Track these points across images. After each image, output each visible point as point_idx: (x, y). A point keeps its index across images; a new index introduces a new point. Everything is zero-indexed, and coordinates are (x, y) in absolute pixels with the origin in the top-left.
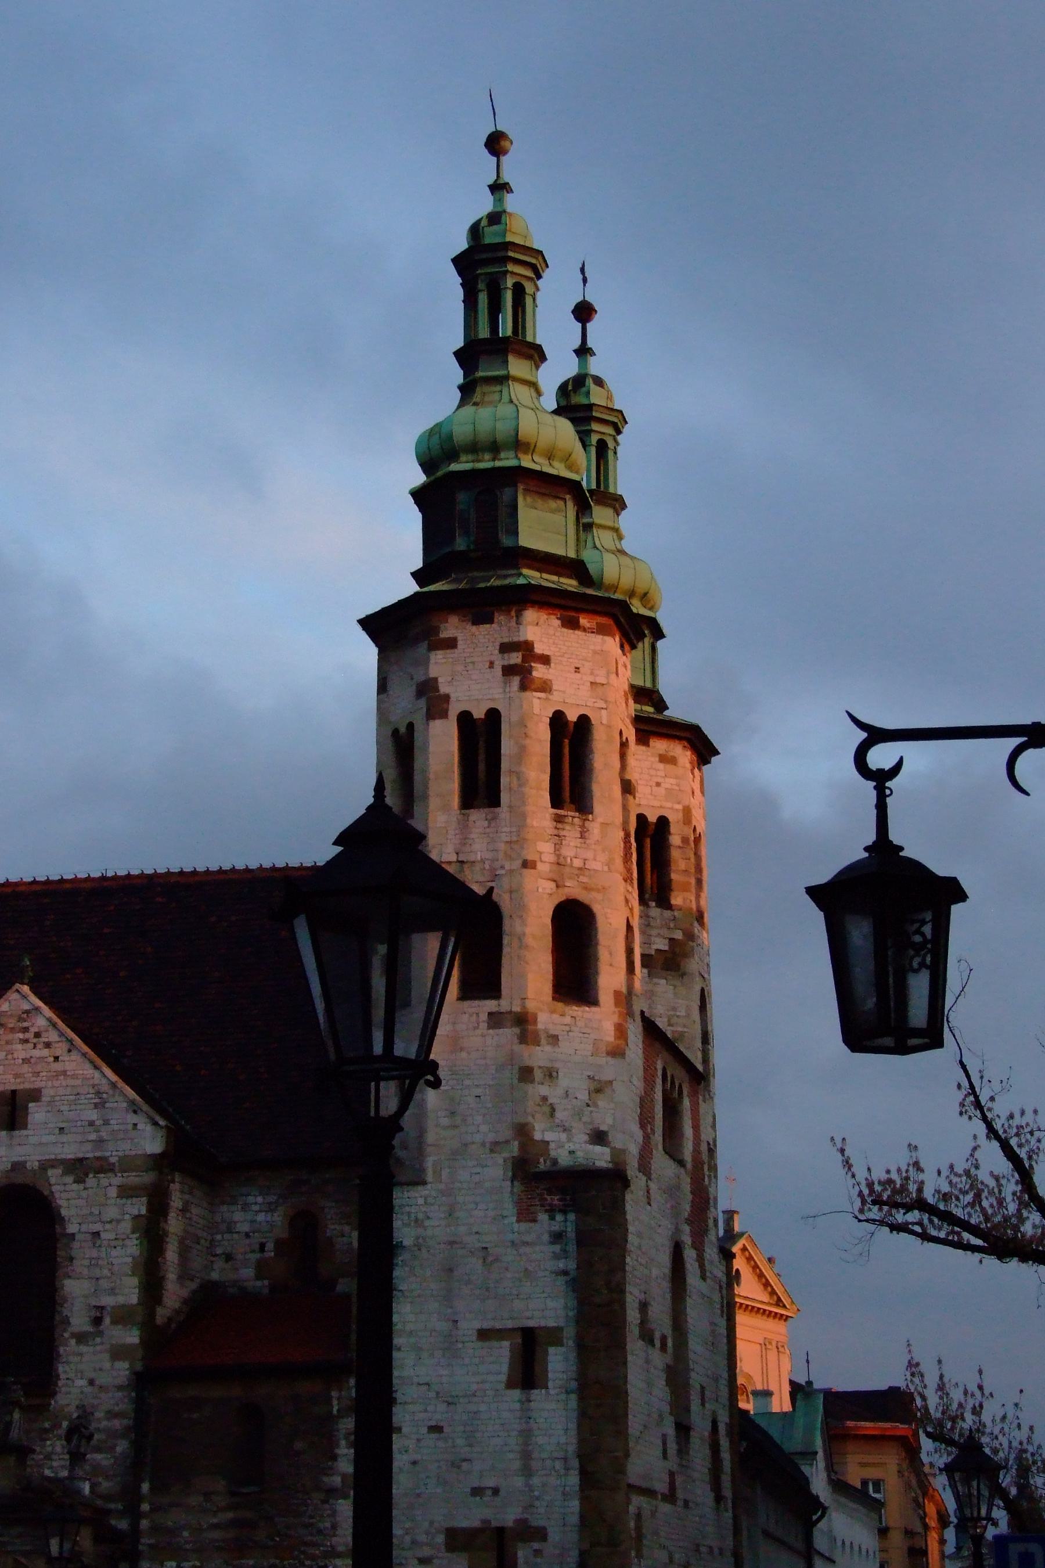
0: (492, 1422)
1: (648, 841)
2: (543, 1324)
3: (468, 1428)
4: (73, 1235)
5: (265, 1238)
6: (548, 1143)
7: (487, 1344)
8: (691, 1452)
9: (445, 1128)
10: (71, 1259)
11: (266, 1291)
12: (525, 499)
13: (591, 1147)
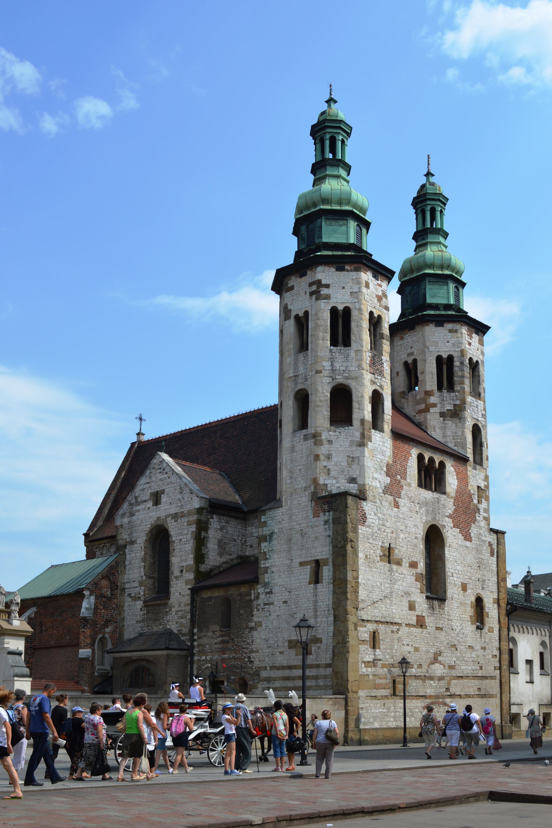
0: (304, 598)
2: (321, 558)
3: (296, 601)
7: (302, 568)
10: (174, 550)
12: (326, 223)
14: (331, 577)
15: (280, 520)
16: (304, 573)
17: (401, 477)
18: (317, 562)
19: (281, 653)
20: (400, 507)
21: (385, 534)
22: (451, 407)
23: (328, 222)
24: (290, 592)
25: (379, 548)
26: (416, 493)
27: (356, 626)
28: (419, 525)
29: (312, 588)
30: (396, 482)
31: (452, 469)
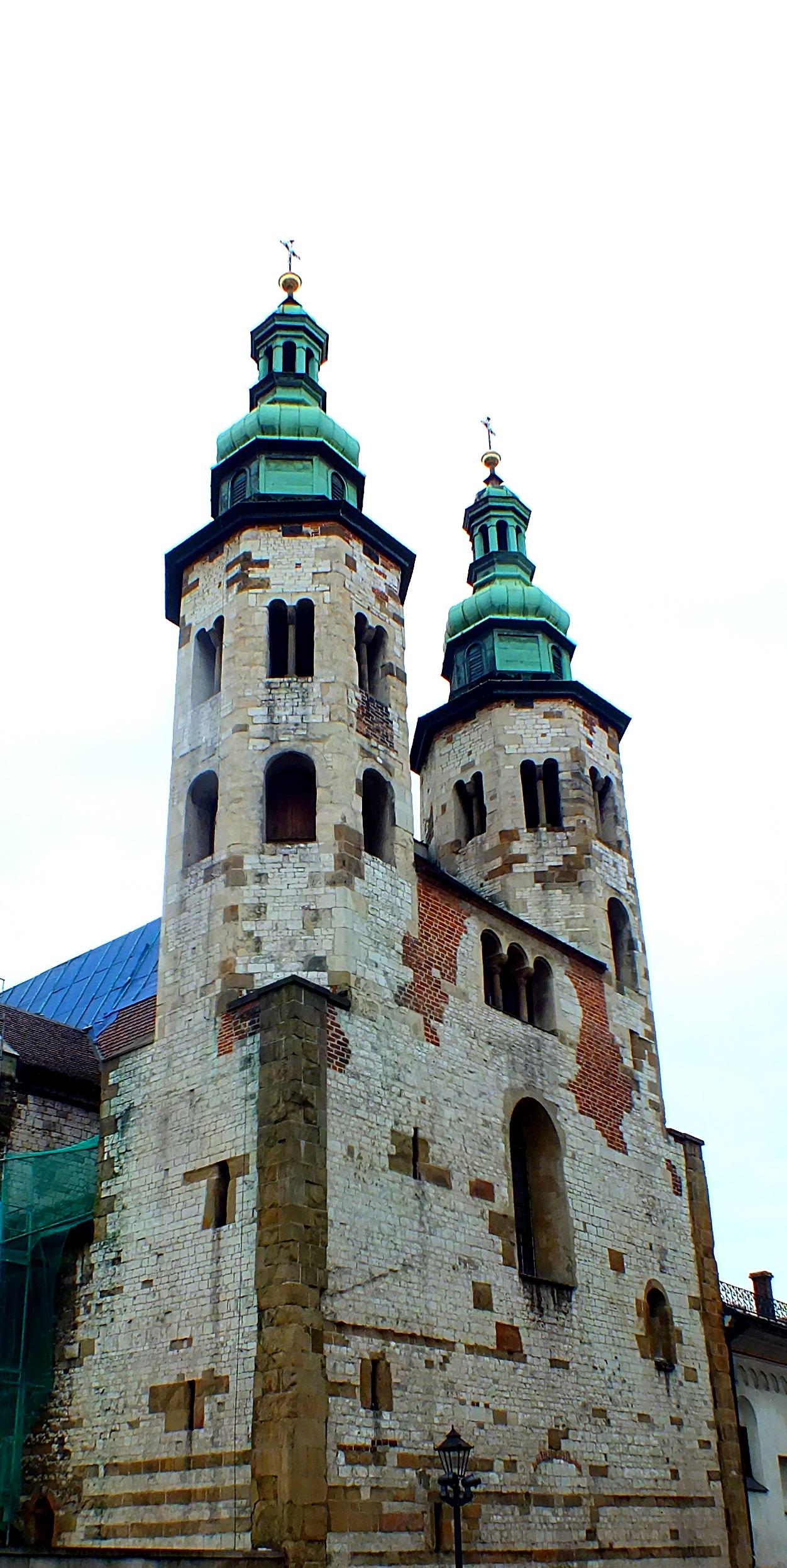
1: (540, 786)
2: (233, 1155)
3: (172, 1278)
6: (252, 974)
7: (189, 1187)
8: (574, 1312)
13: (305, 973)
14: (253, 1204)
15: (148, 1074)
17: (441, 973)
18: (223, 1167)
19: (133, 1425)
20: (441, 1043)
21: (402, 1100)
22: (558, 862)
23: (272, 465)
24: (159, 1255)
25: (386, 1135)
26: (482, 1018)
27: (318, 1340)
28: (492, 1093)
29: (210, 1239)
30: (430, 983)
31: (567, 980)
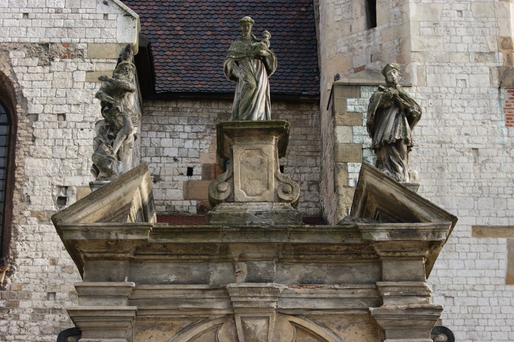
4: (37, 115)
5: (191, 162)
7: (482, 240)
9: (429, 36)
10: (34, 139)
11: (194, 211)
16: (490, 255)
24: (446, 297)
